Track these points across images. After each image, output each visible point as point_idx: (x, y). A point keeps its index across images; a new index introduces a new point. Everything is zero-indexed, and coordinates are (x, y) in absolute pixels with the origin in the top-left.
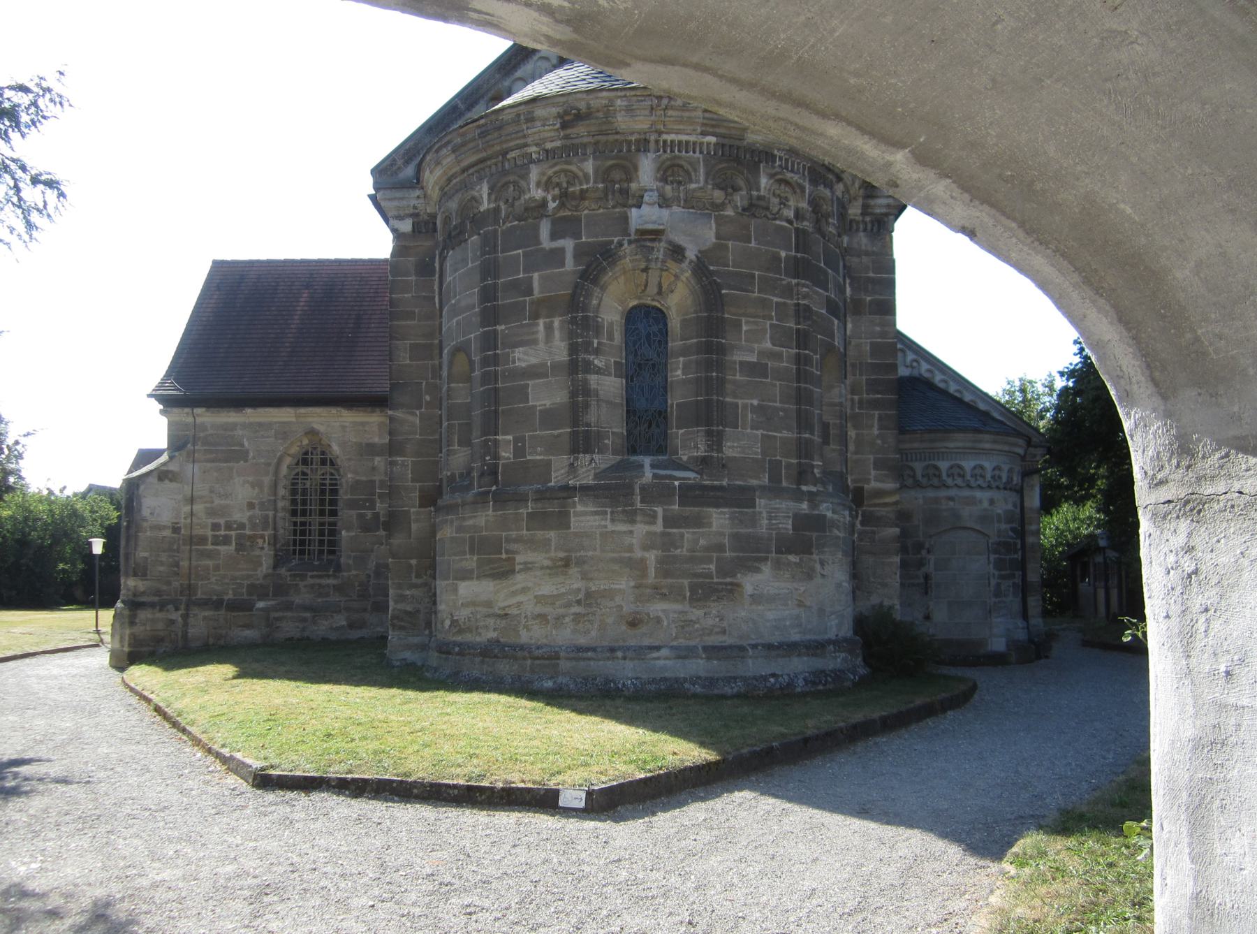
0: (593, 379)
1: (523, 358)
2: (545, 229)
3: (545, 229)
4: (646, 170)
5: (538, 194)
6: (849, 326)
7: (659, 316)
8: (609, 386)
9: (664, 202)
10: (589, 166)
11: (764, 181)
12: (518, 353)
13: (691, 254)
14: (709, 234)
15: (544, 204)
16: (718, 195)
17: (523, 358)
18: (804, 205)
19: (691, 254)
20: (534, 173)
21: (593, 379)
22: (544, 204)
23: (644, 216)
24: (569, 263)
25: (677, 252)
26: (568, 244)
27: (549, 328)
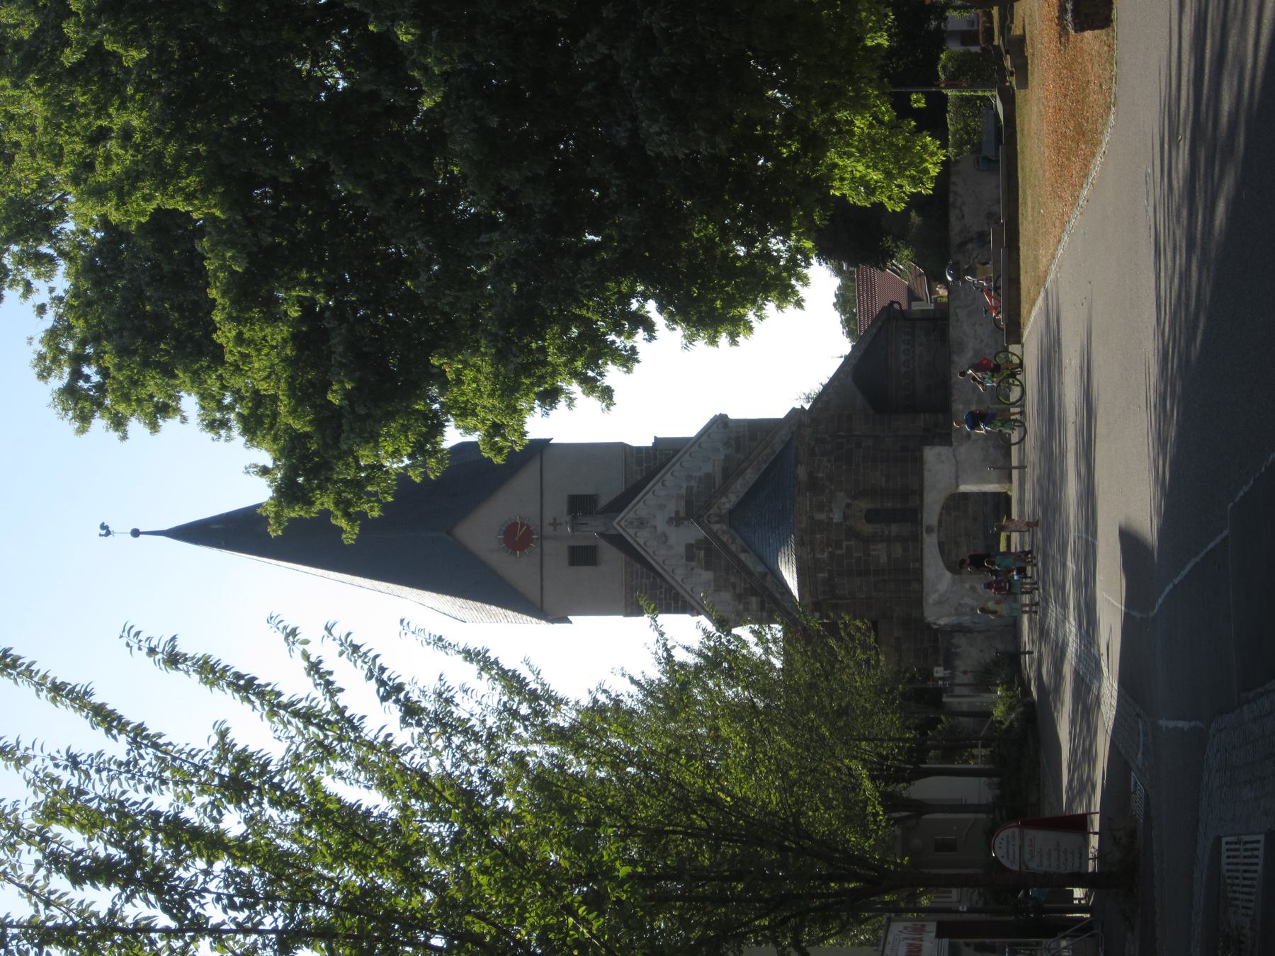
0: (893, 534)
1: (884, 559)
2: (839, 552)
3: (839, 552)
4: (821, 516)
5: (826, 555)
6: (857, 433)
7: (869, 511)
8: (894, 529)
9: (831, 510)
10: (818, 536)
11: (820, 475)
12: (881, 561)
13: (849, 501)
14: (841, 495)
15: (830, 552)
16: (827, 491)
17: (884, 559)
18: (825, 459)
19: (849, 501)
20: (819, 556)
21: (893, 534)
22: (830, 552)
23: (837, 517)
24: (852, 543)
25: (848, 506)
26: (845, 544)
27: (874, 550)
